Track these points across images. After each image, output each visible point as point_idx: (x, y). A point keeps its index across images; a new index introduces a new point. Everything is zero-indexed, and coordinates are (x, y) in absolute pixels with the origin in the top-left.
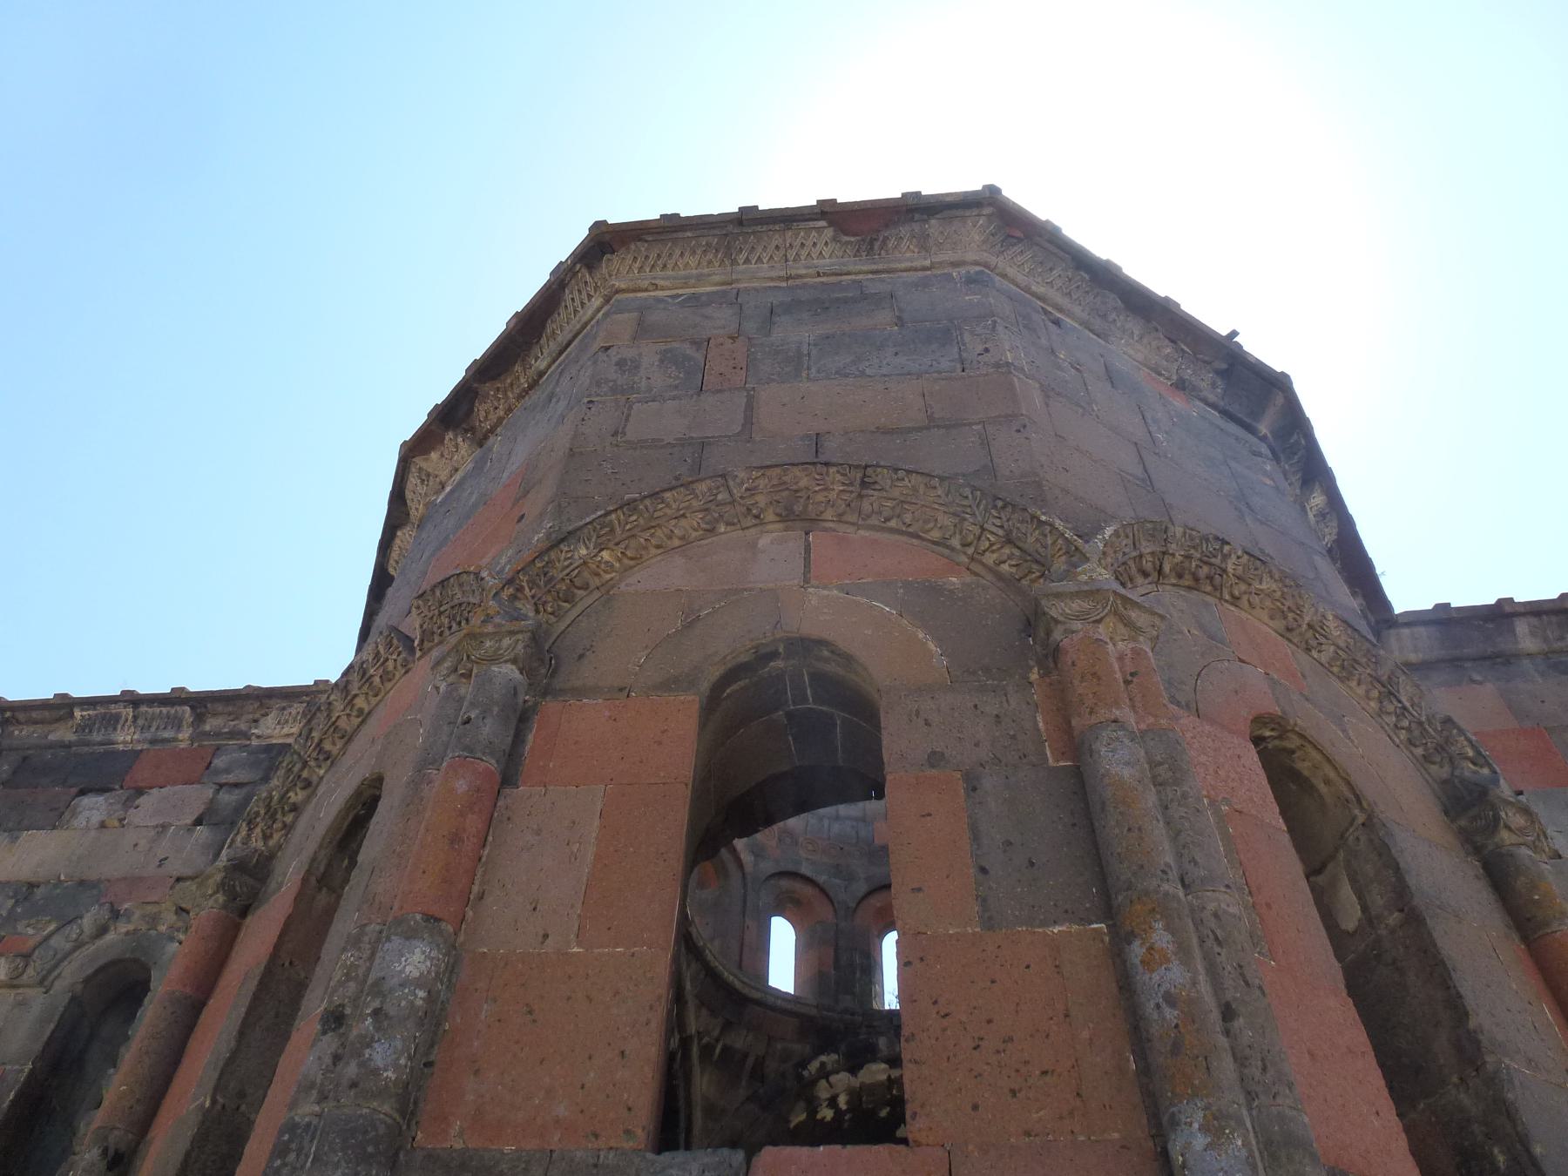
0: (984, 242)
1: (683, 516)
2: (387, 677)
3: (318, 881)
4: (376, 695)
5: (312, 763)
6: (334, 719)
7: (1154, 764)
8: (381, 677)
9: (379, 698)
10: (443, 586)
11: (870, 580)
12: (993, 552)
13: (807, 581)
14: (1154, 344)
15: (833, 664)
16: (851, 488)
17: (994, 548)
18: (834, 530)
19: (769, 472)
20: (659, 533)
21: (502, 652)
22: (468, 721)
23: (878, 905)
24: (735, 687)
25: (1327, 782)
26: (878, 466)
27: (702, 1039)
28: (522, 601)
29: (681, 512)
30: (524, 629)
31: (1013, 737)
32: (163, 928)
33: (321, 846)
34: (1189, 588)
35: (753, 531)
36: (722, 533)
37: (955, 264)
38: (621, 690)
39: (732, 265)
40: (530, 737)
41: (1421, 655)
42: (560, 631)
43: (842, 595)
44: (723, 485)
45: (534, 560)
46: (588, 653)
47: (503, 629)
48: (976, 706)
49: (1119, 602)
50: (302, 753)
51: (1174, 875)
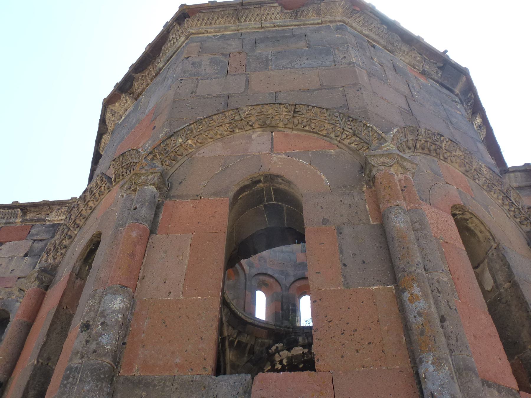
0: (343, 12)
1: (221, 125)
2: (101, 194)
3: (76, 275)
4: (97, 201)
5: (72, 229)
6: (80, 211)
7: (413, 223)
8: (99, 193)
9: (98, 202)
10: (123, 156)
11: (298, 151)
12: (348, 139)
14: (413, 55)
15: (283, 185)
16: (289, 114)
17: (348, 137)
18: (283, 131)
19: (256, 107)
20: (211, 133)
22: (136, 209)
23: (298, 286)
24: (244, 194)
25: (481, 232)
26: (301, 104)
27: (230, 338)
28: (156, 161)
29: (220, 124)
31: (356, 213)
32: (14, 297)
33: (77, 262)
34: (427, 154)
35: (250, 131)
36: (237, 133)
37: (331, 22)
38: (198, 196)
39: (239, 22)
40: (161, 215)
41: (518, 184)
42: (171, 173)
43: (286, 157)
44: (237, 113)
45: (160, 144)
47: (149, 172)
48: (341, 201)
49: (399, 158)
50: (68, 225)
51: (421, 266)
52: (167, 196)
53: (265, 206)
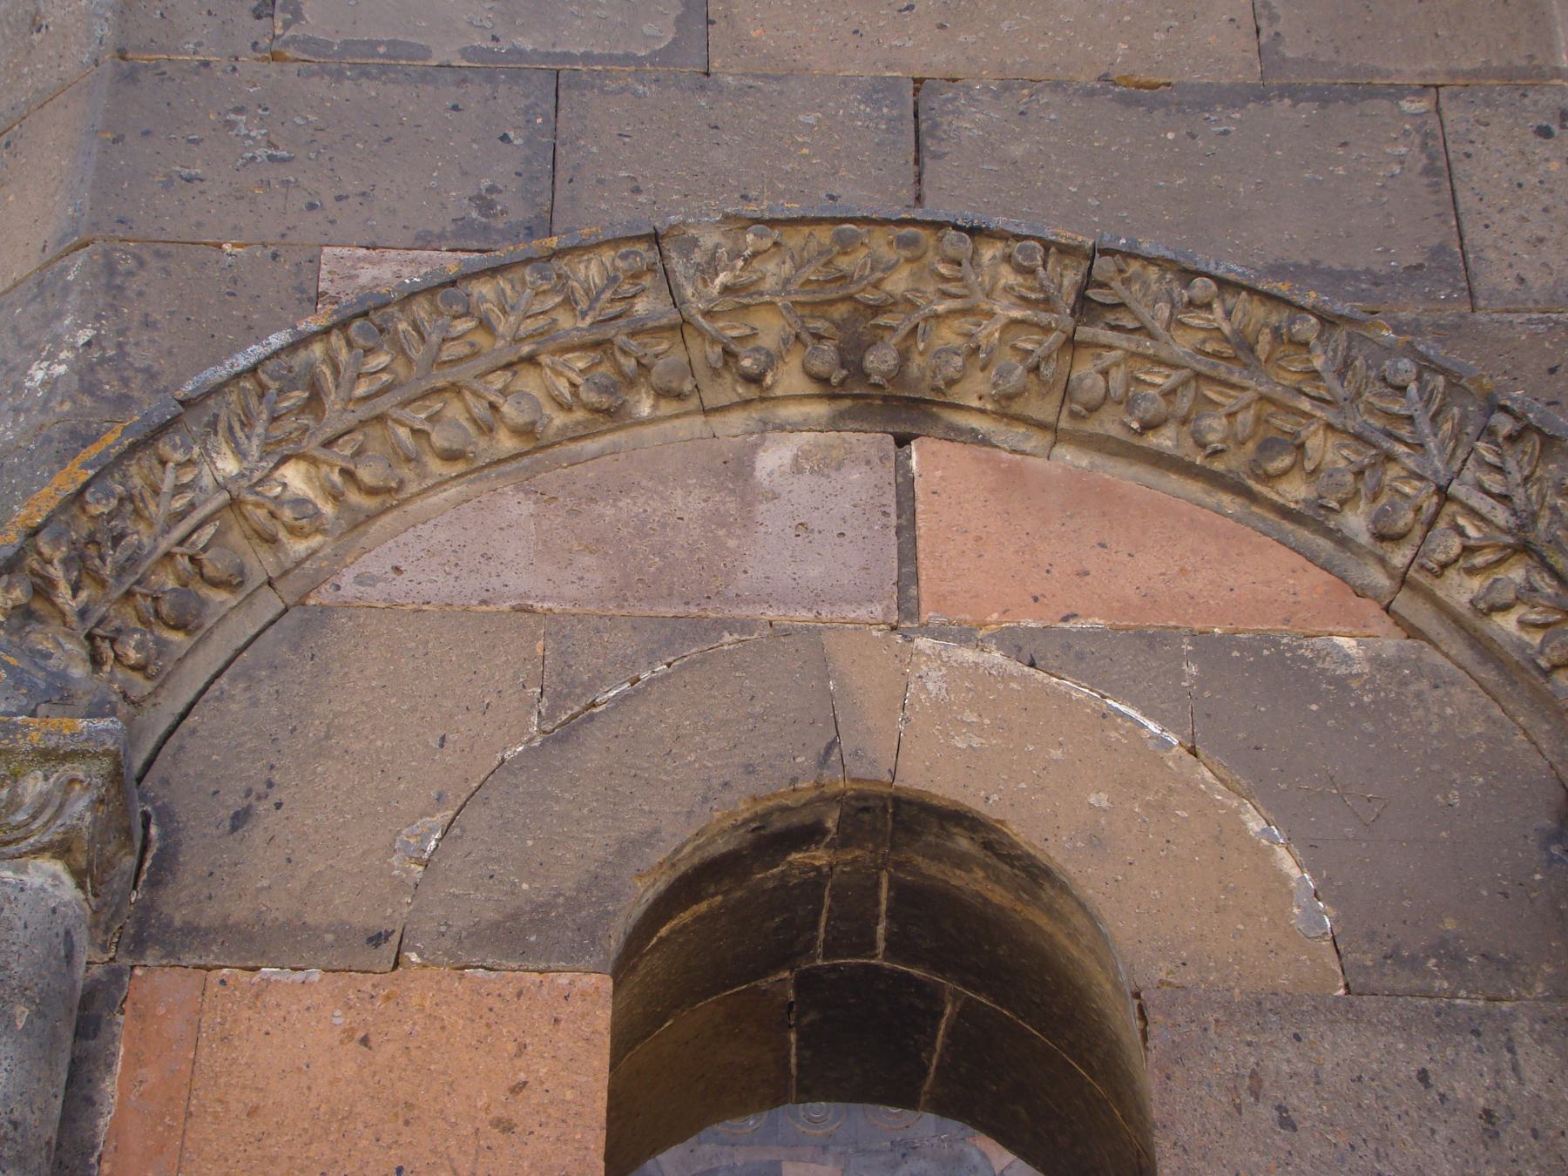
1: (531, 360)
11: (1098, 622)
12: (1471, 571)
13: (908, 606)
15: (980, 874)
16: (1044, 317)
17: (1479, 560)
19: (795, 239)
20: (455, 410)
21: (21, 817)
24: (685, 917)
26: (1129, 255)
28: (50, 631)
29: (526, 349)
30: (90, 746)
35: (736, 421)
36: (641, 422)
38: (377, 939)
40: (110, 1087)
43: (1015, 668)
44: (651, 269)
45: (81, 492)
46: (261, 808)
47: (23, 744)
48: (1423, 1076)
52: (141, 923)
53: (806, 982)
